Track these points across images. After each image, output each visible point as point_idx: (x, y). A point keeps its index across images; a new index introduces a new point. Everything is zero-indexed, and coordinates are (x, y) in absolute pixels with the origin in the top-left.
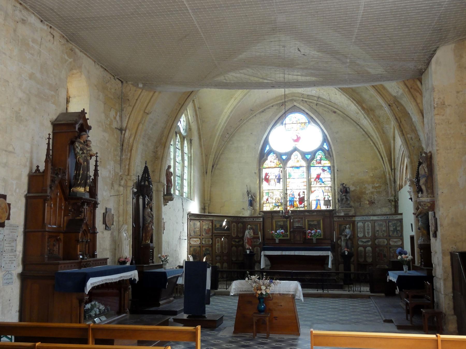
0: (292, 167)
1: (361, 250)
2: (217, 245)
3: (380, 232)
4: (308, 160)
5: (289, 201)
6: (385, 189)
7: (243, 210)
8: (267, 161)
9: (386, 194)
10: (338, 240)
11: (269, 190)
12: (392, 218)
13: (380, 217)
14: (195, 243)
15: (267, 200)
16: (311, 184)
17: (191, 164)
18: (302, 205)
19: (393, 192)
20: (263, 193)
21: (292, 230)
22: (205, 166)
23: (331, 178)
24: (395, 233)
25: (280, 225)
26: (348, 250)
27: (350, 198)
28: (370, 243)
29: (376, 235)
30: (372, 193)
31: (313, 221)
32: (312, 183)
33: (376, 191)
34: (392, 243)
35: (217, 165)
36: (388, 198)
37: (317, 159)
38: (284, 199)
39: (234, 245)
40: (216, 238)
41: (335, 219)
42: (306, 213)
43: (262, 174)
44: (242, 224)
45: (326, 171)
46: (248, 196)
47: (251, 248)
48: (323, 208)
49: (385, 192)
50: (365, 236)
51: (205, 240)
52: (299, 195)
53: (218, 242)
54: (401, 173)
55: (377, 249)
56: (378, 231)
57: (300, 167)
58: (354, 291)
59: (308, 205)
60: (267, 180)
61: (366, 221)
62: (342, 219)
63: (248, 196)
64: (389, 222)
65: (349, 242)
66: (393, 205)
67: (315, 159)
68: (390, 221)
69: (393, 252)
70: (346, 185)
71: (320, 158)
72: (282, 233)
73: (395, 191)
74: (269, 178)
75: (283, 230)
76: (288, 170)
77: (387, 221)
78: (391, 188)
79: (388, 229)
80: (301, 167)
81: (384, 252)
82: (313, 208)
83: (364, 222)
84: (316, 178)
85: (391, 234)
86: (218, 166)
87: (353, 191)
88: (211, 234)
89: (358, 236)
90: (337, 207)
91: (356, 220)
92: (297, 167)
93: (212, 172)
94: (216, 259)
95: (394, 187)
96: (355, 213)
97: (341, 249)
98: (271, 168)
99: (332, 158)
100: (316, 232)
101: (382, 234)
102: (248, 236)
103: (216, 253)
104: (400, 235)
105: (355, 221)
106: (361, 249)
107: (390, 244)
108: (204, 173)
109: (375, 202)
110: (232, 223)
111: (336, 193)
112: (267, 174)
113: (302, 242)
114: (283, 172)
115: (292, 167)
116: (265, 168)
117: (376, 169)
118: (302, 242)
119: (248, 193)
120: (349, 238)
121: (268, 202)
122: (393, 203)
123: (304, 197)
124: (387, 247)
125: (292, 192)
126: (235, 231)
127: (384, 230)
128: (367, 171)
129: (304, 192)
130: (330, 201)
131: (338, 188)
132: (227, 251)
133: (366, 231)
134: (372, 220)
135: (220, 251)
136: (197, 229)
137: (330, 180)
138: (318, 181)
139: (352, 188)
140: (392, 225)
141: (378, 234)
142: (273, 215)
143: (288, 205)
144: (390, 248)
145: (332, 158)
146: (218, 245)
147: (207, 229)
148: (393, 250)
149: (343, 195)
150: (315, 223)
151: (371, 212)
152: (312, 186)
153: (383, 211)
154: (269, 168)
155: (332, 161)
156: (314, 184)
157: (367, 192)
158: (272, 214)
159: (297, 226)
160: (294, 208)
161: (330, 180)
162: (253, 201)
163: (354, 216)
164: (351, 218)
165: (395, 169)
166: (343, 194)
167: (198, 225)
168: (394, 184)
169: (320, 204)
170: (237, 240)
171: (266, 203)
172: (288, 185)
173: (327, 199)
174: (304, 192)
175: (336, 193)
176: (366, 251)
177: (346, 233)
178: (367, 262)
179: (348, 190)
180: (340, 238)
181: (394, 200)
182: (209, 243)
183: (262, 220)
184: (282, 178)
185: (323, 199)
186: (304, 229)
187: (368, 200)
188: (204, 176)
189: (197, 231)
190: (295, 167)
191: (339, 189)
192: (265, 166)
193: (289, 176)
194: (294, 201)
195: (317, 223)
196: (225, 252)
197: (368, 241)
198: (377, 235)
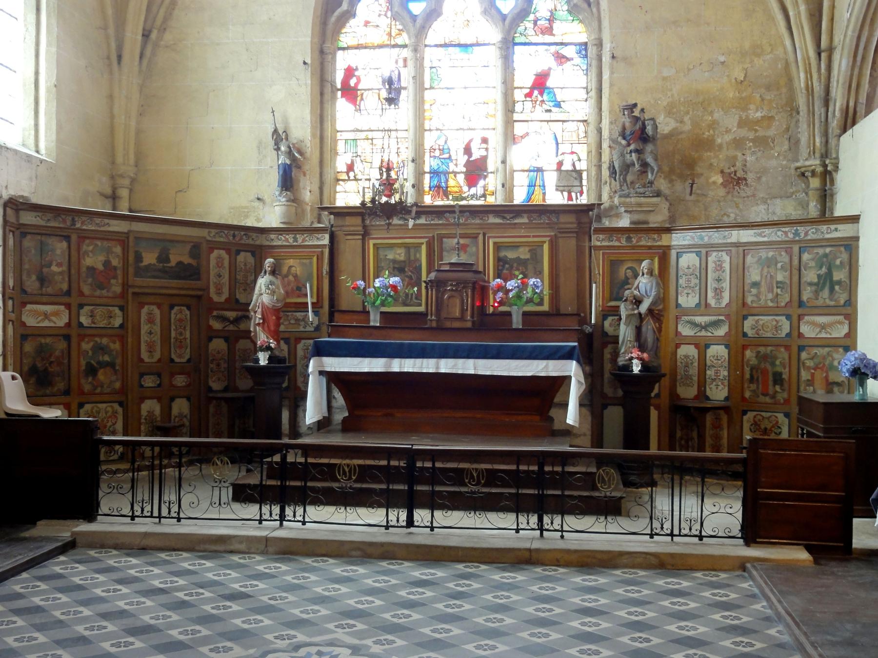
0: (445, 45)
1: (686, 357)
2: (145, 328)
3: (763, 289)
4: (504, 17)
5: (430, 173)
6: (788, 129)
7: (257, 204)
8: (352, 22)
9: (790, 149)
10: (605, 317)
11: (358, 130)
12: (815, 237)
13: (767, 231)
14: (46, 324)
15: (350, 168)
16: (512, 111)
17: (38, 9)
18: (478, 190)
19: (818, 140)
20: (335, 141)
21: (433, 275)
22: (111, 31)
23: (586, 88)
24: (826, 293)
25: (394, 261)
26: (645, 355)
27: (656, 160)
28: (722, 331)
29: (749, 300)
30: (738, 143)
31: (515, 247)
32: (518, 107)
33: (751, 135)
34: (806, 330)
35: (163, 30)
36: (798, 164)
37: (538, 15)
38: (410, 163)
39: (218, 331)
40: (142, 305)
41: (598, 241)
42: (491, 216)
43: (334, 70)
44: (253, 254)
45: (568, 63)
46: (278, 149)
47: (272, 345)
48: (555, 198)
49: (787, 142)
50: (707, 305)
51: (92, 311)
52: (468, 150)
53: (151, 321)
54: (858, 63)
55: (748, 353)
56: (756, 284)
57: (472, 45)
58: (672, 535)
59: (499, 187)
60: (351, 93)
61: (712, 247)
62: (624, 242)
63: (278, 149)
65: (649, 327)
66: (817, 189)
67: (532, 17)
68: (805, 246)
69: (810, 363)
70: (642, 110)
71: (551, 12)
72: (394, 287)
73: (826, 134)
74: (359, 87)
75: (397, 279)
76: (430, 55)
77: (796, 249)
78: (811, 124)
79: (795, 278)
80: (478, 45)
81: (778, 362)
82: (519, 197)
83: (704, 251)
84: (532, 89)
85: (811, 295)
86: (168, 37)
87: (668, 137)
88: (118, 289)
89: (678, 305)
90: (605, 197)
91: (673, 243)
92: (465, 46)
93: (142, 56)
94: (142, 386)
95: (823, 119)
96: (672, 218)
97: (616, 354)
98: (366, 47)
99: (594, 10)
100: (524, 285)
101: (770, 296)
102: (266, 299)
103: (142, 360)
104: (842, 302)
105: (669, 247)
106: (687, 351)
107: (800, 335)
108: (108, 58)
109: (745, 179)
110: (211, 250)
111: (605, 145)
112: (350, 72)
113: (469, 325)
114: (410, 63)
115: (445, 45)
116: (344, 49)
117: (756, 51)
118: (469, 325)
119: (278, 137)
120: (650, 311)
121: (352, 178)
122: (815, 183)
123: (484, 159)
124: (787, 348)
125: (443, 139)
126: (226, 279)
127: (781, 282)
128: (722, 59)
129: (485, 141)
130: (579, 173)
131: (611, 123)
132: (187, 357)
133: (711, 284)
134: (737, 245)
135: (157, 355)
136: (54, 268)
137: (585, 96)
138: (540, 99)
139: (665, 125)
140: (812, 264)
141: (757, 296)
142: (368, 222)
143: (427, 189)
144: (801, 348)
145: (594, 10)
146: (151, 333)
147: (100, 267)
148: (812, 359)
149: (632, 147)
150: (523, 254)
151: (732, 216)
152: (516, 117)
153: (774, 213)
154: (358, 47)
155: (595, 24)
156: (524, 109)
157: (719, 141)
158: (363, 220)
159: (453, 261)
160: (448, 199)
161: (585, 96)
162: (294, 172)
163: (668, 230)
164: (656, 236)
165: (831, 50)
166: (629, 145)
167: (58, 252)
168: (823, 110)
169: (544, 186)
170: (231, 315)
171: (344, 180)
172: (427, 114)
173: (570, 168)
174: (485, 141)
175: (605, 145)
176: (708, 358)
177: (636, 292)
178: (708, 398)
179: (649, 130)
180: (615, 311)
181: (819, 169)
182: (110, 323)
183: (325, 240)
184: (405, 88)
185: (555, 167)
186: (478, 276)
187: (722, 172)
188: (111, 73)
189: (54, 274)
190: (455, 46)
191: (618, 129)
192: (345, 39)
193: (431, 79)
194: (446, 173)
195: (528, 256)
196: (182, 356)
197: (716, 324)
198: (752, 302)
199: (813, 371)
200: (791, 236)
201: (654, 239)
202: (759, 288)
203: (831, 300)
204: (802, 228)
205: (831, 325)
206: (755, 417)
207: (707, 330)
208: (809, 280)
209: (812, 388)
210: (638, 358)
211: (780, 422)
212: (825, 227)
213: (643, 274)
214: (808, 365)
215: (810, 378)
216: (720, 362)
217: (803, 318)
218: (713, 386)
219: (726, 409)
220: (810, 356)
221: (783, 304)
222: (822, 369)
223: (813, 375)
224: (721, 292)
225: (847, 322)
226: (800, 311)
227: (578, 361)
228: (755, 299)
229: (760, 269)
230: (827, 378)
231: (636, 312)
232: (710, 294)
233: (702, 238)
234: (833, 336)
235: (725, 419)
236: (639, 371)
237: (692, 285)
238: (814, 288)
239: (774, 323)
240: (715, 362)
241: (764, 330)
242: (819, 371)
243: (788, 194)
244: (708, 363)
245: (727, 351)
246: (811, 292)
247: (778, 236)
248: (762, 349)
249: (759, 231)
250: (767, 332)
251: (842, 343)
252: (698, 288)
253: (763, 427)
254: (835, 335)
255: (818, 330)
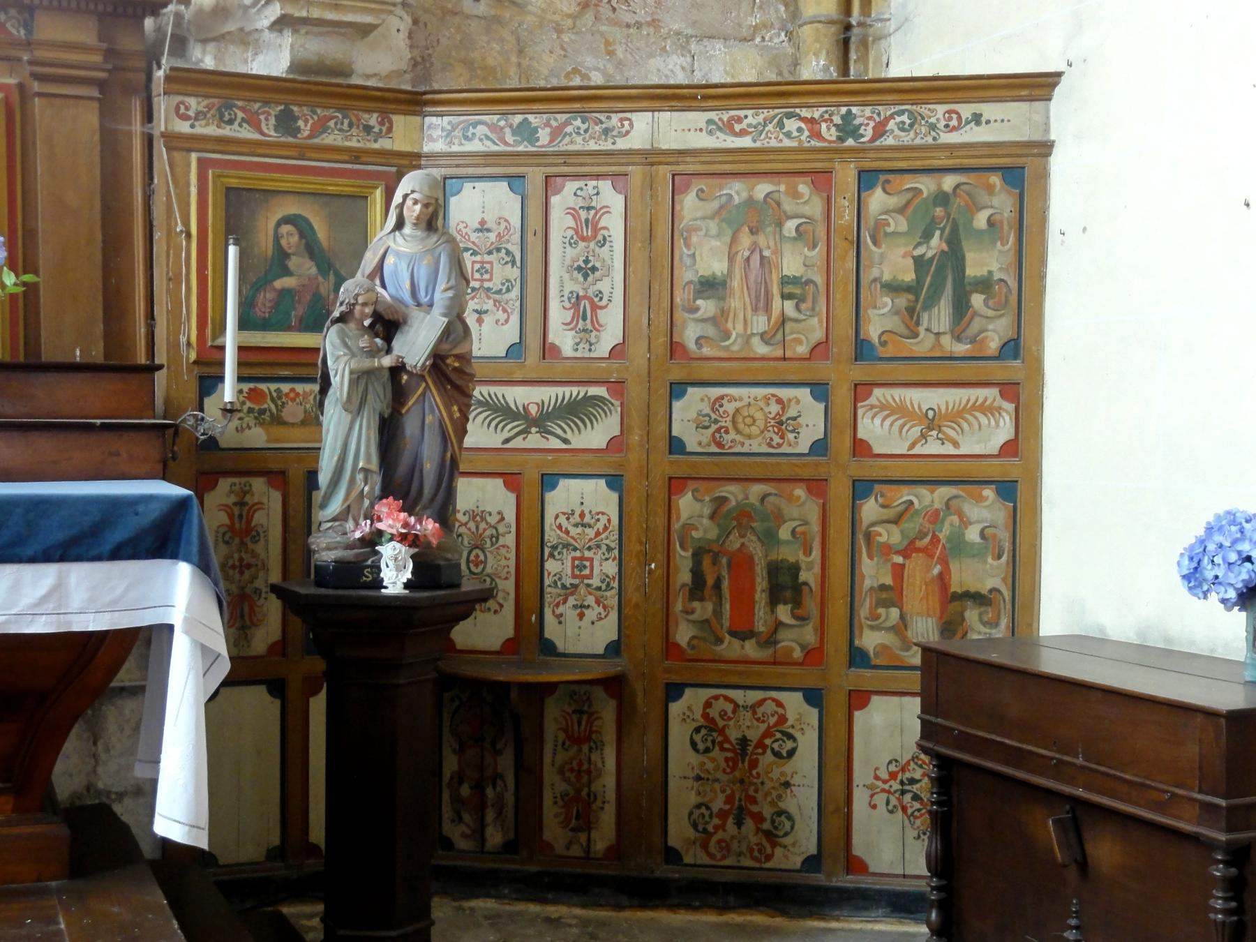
1: (477, 516)
3: (738, 301)
12: (907, 139)
13: (752, 118)
24: (940, 316)
28: (597, 435)
29: (690, 334)
50: (548, 351)
55: (686, 504)
56: (710, 286)
64: (867, 179)
77: (846, 175)
81: (784, 533)
85: (894, 323)
96: (421, 64)
101: (760, 323)
104: (993, 345)
107: (860, 448)
124: (817, 486)
127: (795, 281)
133: (561, 281)
134: (652, 157)
144: (861, 488)
148: (896, 521)
164: (373, 120)
176: (549, 519)
178: (548, 648)
198: (698, 341)
199: (899, 559)
200: (829, 133)
201: (368, 129)
202: (722, 298)
203: (958, 338)
204: (868, 111)
205: (957, 416)
206: (708, 704)
207: (545, 432)
208: (887, 277)
209: (895, 612)
210: (403, 538)
211: (791, 718)
212: (941, 109)
213: (400, 225)
214: (882, 539)
215: (888, 581)
216: (591, 533)
217: (869, 394)
218: (568, 610)
219: (615, 685)
220: (890, 513)
221: (802, 350)
222: (926, 551)
223: (898, 571)
224: (595, 308)
225: (1010, 407)
226: (859, 372)
227: (203, 566)
228: (710, 331)
229: (728, 239)
230: (943, 579)
231: (387, 361)
232: (558, 314)
233: (529, 133)
234: (962, 451)
235: (607, 711)
236: (407, 585)
237: (495, 284)
238: (903, 301)
239: (774, 408)
240: (574, 531)
241: (738, 432)
242: (917, 561)
243: (745, 32)
244: (551, 535)
245: (614, 496)
246: (895, 312)
247: (788, 135)
248: (732, 492)
249: (725, 116)
250: (749, 437)
251: (995, 470)
252: (515, 292)
253: (734, 735)
254: (968, 447)
255: (916, 431)
